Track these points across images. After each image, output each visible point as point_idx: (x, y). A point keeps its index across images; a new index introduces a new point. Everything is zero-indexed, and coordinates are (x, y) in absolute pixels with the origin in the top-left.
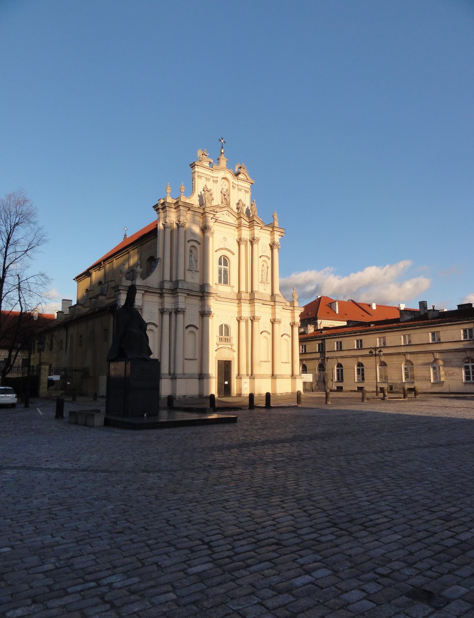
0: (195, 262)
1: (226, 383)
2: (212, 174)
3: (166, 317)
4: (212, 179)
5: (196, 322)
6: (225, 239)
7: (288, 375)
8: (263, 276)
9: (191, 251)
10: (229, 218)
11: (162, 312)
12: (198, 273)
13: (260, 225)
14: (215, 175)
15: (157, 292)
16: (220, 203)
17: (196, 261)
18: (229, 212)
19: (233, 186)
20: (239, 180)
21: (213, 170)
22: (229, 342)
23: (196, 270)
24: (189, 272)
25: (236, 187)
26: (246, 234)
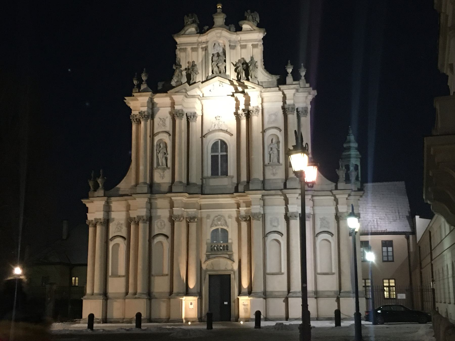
1: (226, 303)
7: (331, 291)
16: (210, 74)
22: (226, 250)
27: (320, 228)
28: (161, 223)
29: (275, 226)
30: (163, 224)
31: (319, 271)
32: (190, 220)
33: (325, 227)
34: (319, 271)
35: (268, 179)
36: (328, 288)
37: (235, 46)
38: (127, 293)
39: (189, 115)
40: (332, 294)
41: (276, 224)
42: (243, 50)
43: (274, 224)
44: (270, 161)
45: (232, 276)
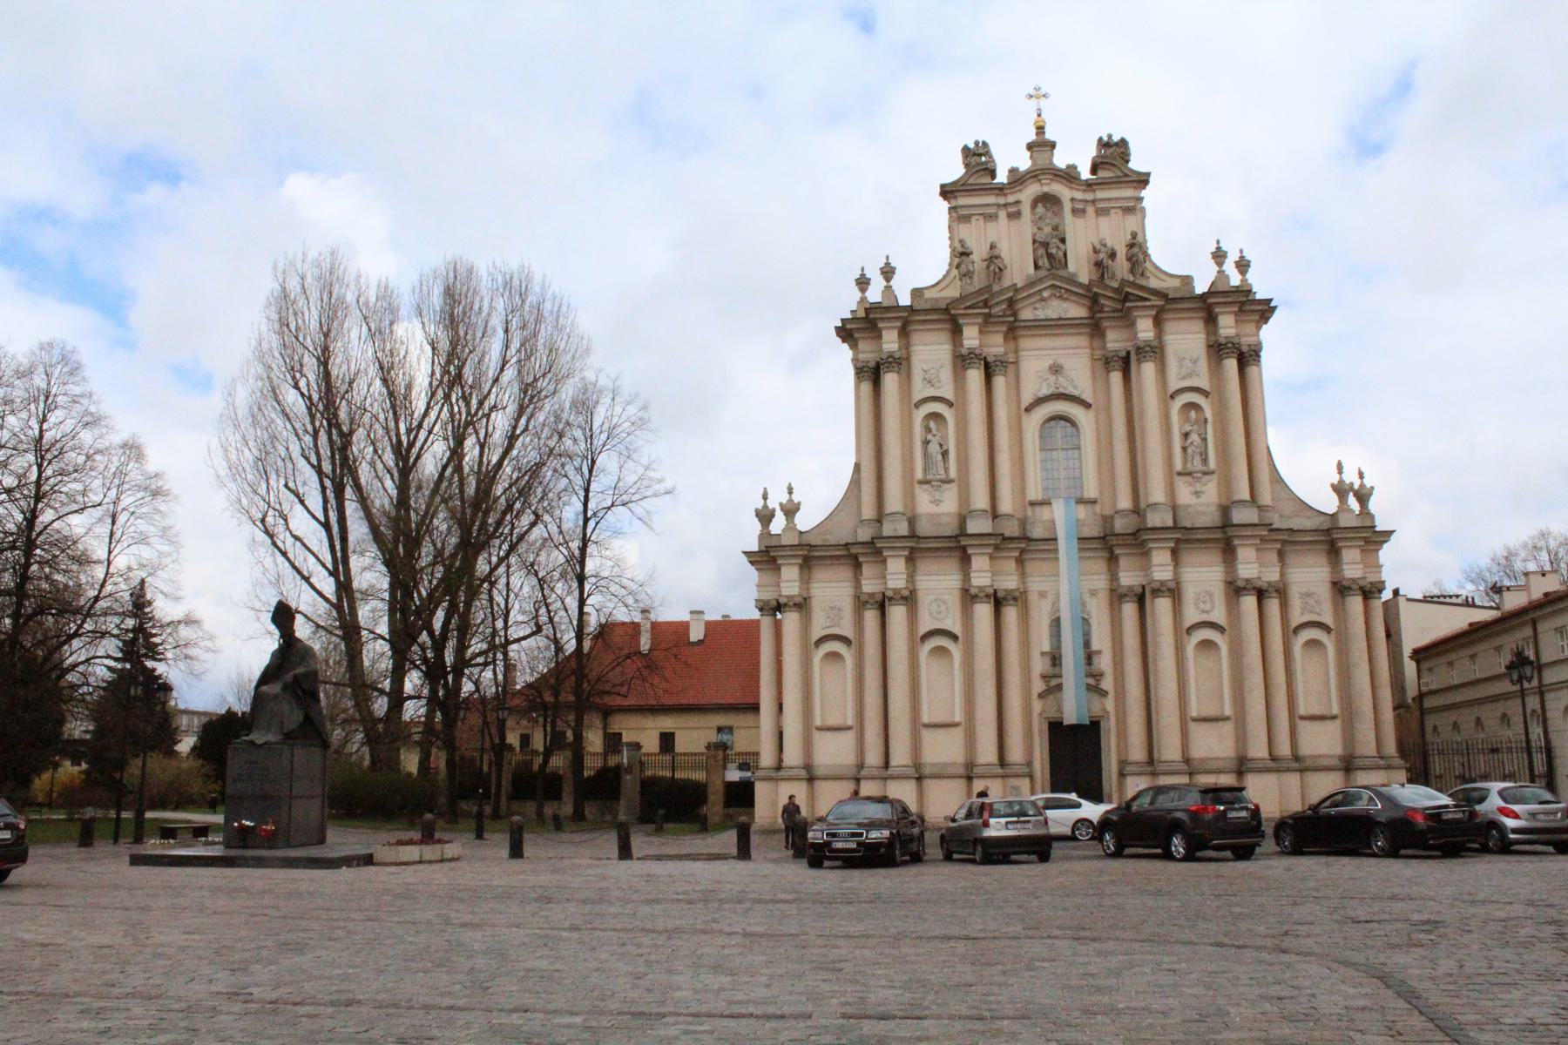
0: (940, 457)
2: (1002, 201)
3: (871, 617)
4: (1002, 214)
5: (953, 623)
6: (1056, 369)
8: (1190, 451)
9: (928, 430)
10: (1065, 305)
11: (860, 603)
12: (953, 485)
13: (1148, 303)
14: (1011, 199)
15: (837, 553)
17: (945, 454)
18: (1061, 288)
19: (1074, 211)
20: (1094, 187)
21: (1001, 189)
23: (943, 477)
24: (925, 486)
25: (1090, 210)
26: (1115, 340)
27: (1303, 614)
28: (939, 606)
29: (1207, 612)
30: (943, 607)
31: (1302, 711)
32: (998, 602)
33: (1311, 612)
34: (1302, 711)
35: (1187, 506)
36: (1323, 750)
37: (1084, 211)
38: (861, 766)
39: (990, 359)
40: (1335, 762)
41: (1208, 607)
42: (1103, 220)
43: (1202, 606)
44: (1185, 462)
45: (1102, 723)
